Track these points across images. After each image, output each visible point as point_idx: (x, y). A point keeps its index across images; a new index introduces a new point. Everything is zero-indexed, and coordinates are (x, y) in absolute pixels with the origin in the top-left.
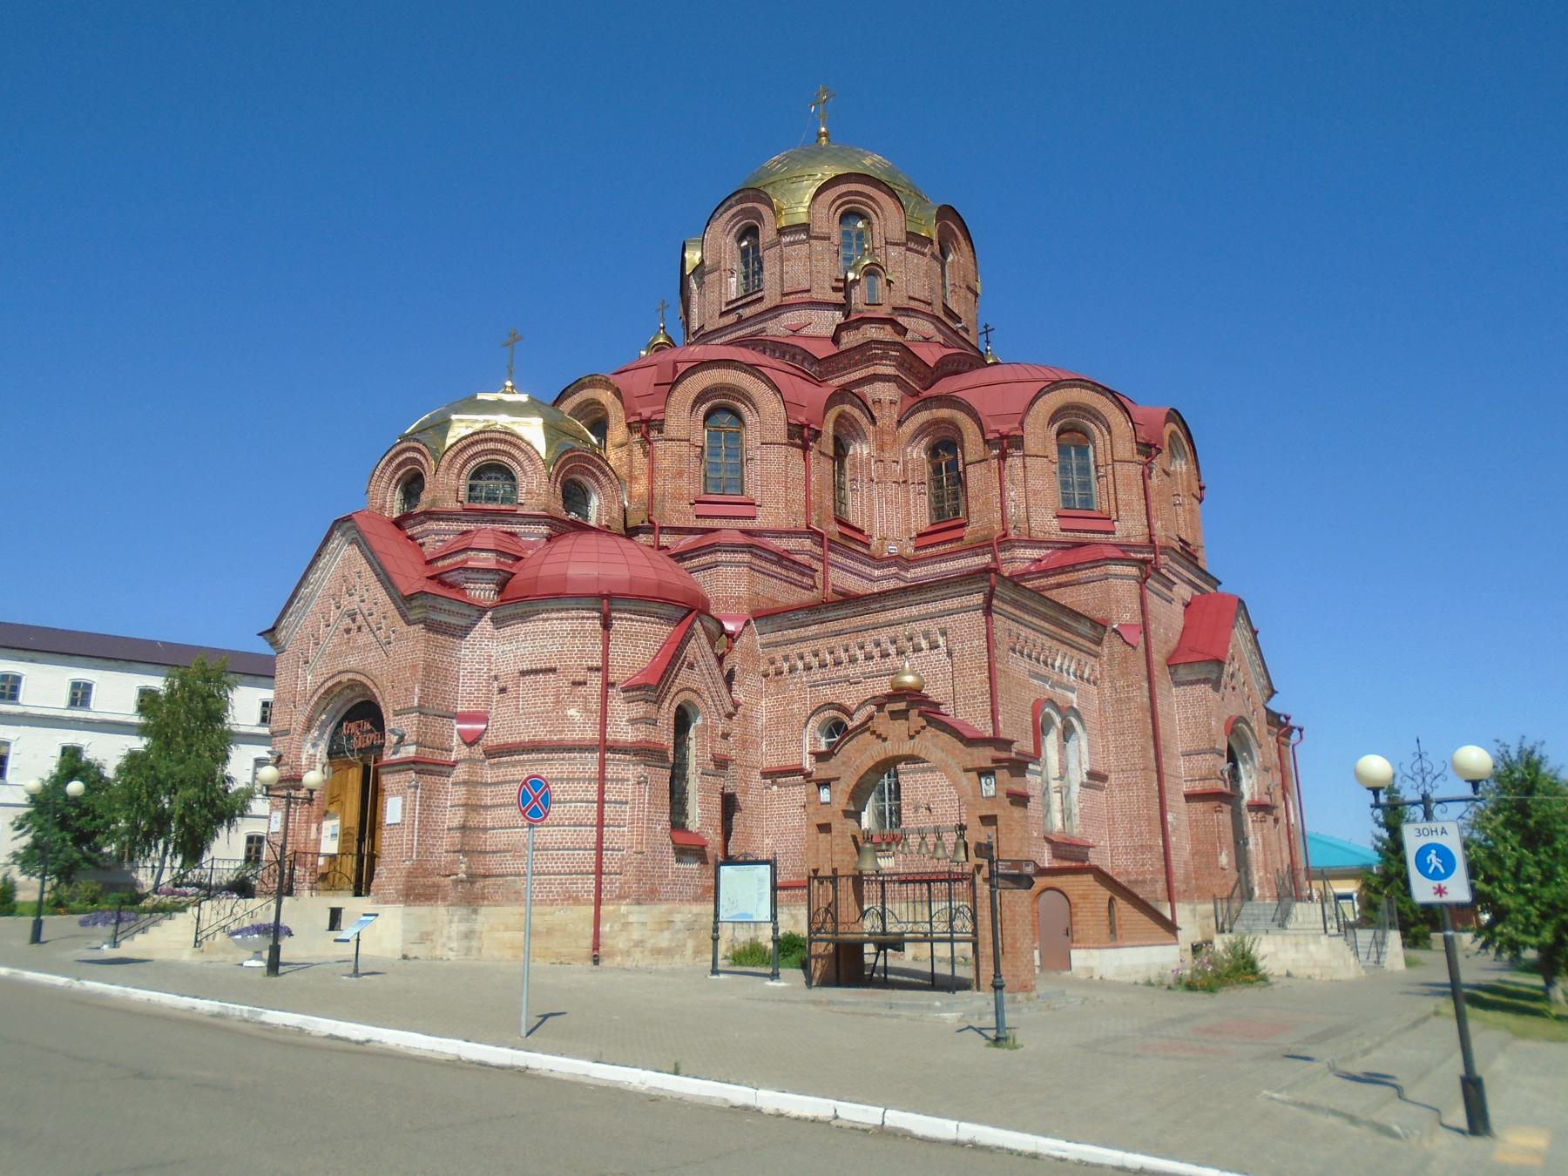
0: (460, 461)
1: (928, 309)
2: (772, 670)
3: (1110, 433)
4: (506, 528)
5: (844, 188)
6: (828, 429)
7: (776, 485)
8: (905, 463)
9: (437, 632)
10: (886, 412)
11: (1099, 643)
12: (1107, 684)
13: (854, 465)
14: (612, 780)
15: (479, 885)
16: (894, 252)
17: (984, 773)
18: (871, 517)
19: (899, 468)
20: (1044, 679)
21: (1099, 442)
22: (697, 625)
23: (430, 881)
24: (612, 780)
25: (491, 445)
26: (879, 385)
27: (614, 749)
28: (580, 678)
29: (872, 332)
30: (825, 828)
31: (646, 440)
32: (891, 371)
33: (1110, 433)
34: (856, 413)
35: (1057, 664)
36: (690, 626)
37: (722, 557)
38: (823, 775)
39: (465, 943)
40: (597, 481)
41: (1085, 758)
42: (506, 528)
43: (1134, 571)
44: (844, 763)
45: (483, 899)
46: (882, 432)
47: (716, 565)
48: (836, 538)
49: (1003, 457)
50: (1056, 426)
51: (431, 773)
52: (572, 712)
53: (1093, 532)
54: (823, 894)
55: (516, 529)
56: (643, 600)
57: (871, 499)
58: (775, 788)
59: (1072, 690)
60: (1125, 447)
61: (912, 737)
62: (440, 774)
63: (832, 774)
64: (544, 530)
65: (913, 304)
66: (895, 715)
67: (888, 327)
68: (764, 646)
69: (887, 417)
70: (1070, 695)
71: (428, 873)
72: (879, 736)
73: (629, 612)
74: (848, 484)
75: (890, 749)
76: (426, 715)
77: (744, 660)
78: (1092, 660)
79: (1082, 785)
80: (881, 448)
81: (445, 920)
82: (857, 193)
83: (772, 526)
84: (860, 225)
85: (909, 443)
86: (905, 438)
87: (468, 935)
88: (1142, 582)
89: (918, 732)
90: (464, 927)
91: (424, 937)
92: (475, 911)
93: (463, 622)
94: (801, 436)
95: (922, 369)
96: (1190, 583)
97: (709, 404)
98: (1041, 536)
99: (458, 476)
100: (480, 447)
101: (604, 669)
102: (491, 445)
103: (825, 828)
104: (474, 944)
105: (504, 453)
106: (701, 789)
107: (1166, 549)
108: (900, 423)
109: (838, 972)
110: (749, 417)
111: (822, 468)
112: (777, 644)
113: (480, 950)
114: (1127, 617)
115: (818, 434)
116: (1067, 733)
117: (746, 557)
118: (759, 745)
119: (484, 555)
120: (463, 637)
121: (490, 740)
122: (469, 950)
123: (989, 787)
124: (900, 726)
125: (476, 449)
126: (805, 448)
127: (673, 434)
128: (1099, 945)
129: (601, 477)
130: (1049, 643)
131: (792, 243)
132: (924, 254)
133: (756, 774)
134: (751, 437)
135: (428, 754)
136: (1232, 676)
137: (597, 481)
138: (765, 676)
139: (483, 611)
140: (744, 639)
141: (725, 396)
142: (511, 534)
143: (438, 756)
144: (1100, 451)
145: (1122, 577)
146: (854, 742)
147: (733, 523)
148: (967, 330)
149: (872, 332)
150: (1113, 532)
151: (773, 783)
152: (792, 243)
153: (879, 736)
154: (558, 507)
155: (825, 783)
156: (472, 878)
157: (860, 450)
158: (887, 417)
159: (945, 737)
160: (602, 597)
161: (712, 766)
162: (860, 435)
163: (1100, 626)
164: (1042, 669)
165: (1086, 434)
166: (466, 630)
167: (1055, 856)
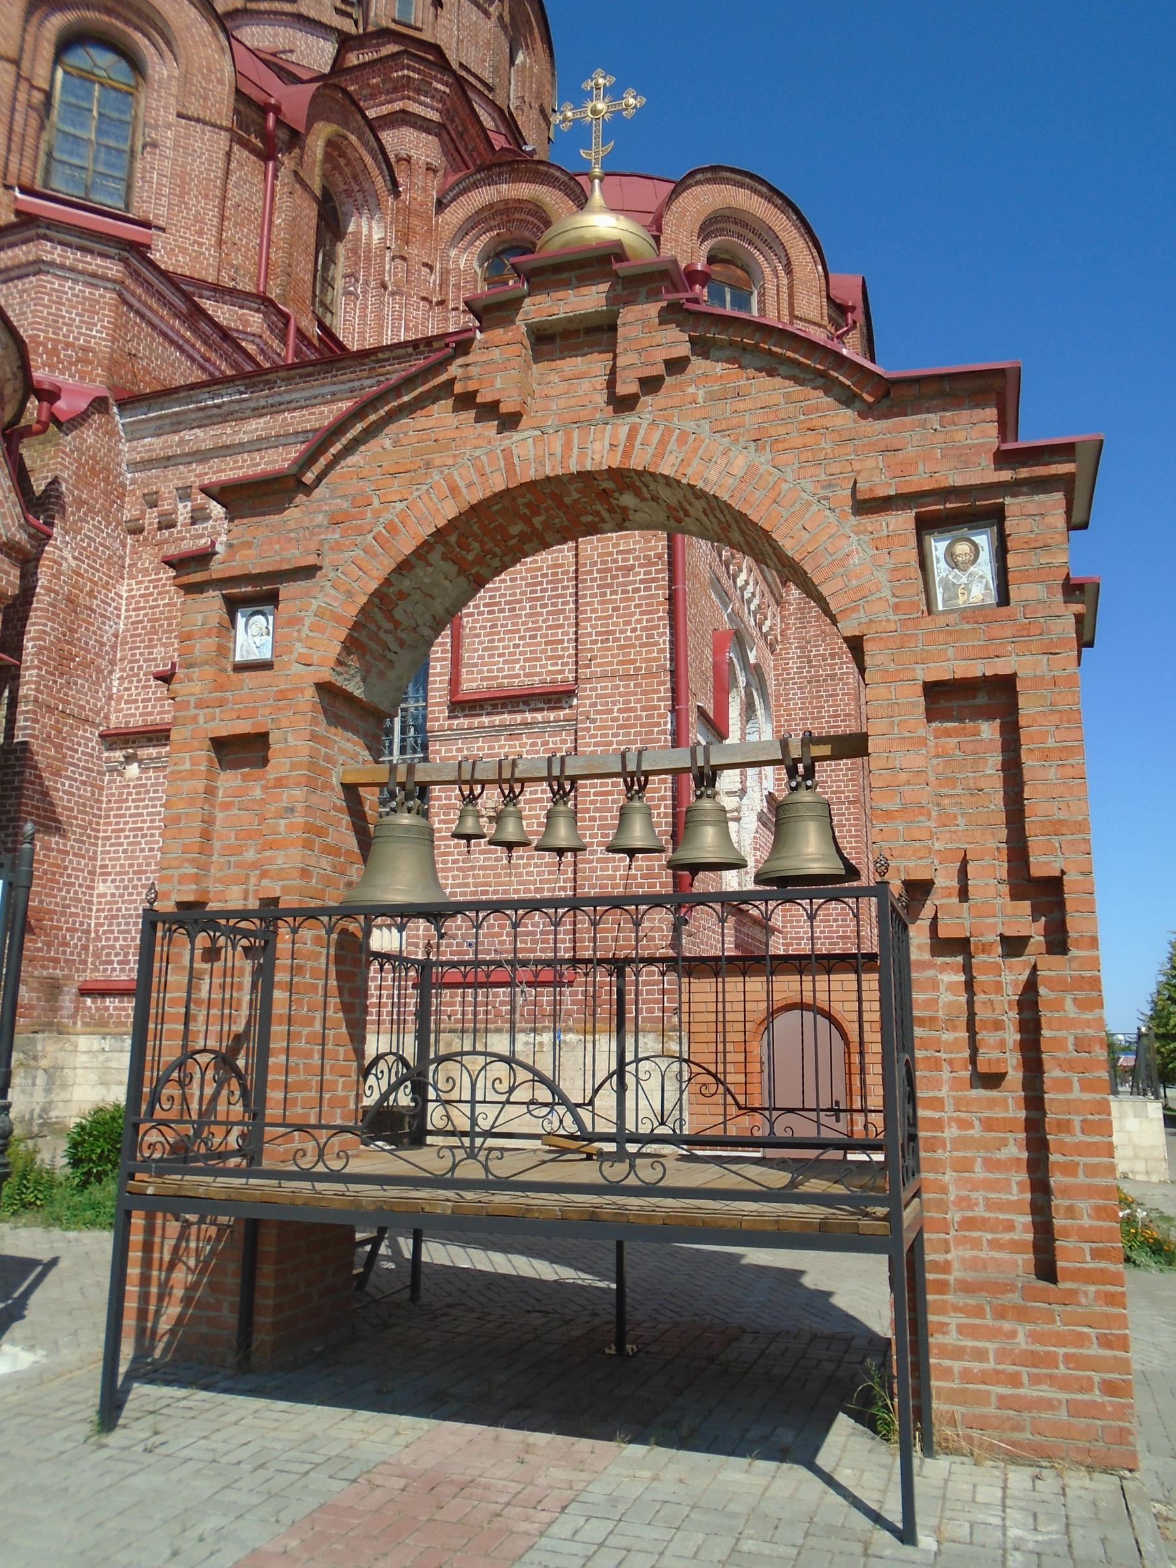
2: (151, 518)
3: (789, 272)
8: (445, 272)
10: (419, 180)
12: (793, 652)
13: (355, 251)
17: (946, 513)
19: (435, 278)
21: (771, 287)
30: (242, 750)
32: (435, 116)
33: (789, 272)
37: (51, 252)
38: (252, 562)
44: (336, 521)
46: (408, 211)
47: (38, 267)
50: (708, 244)
54: (209, 996)
57: (380, 318)
58: (133, 770)
61: (622, 404)
63: (297, 557)
66: (549, 341)
68: (134, 466)
69: (420, 190)
72: (489, 411)
74: (339, 284)
75: (534, 454)
77: (81, 480)
80: (405, 237)
85: (455, 240)
86: (447, 233)
89: (651, 385)
94: (260, 129)
95: (482, 146)
97: (71, 16)
103: (242, 750)
108: (441, 206)
109: (247, 1310)
110: (160, 68)
111: (295, 213)
112: (167, 461)
115: (296, 139)
117: (114, 269)
118: (102, 676)
123: (965, 572)
124: (584, 374)
126: (267, 155)
133: (93, 734)
134: (159, 104)
138: (136, 531)
140: (89, 435)
144: (771, 301)
146: (385, 440)
151: (129, 759)
153: (489, 411)
155: (256, 593)
157: (369, 230)
158: (420, 190)
159: (772, 391)
167: (737, 947)
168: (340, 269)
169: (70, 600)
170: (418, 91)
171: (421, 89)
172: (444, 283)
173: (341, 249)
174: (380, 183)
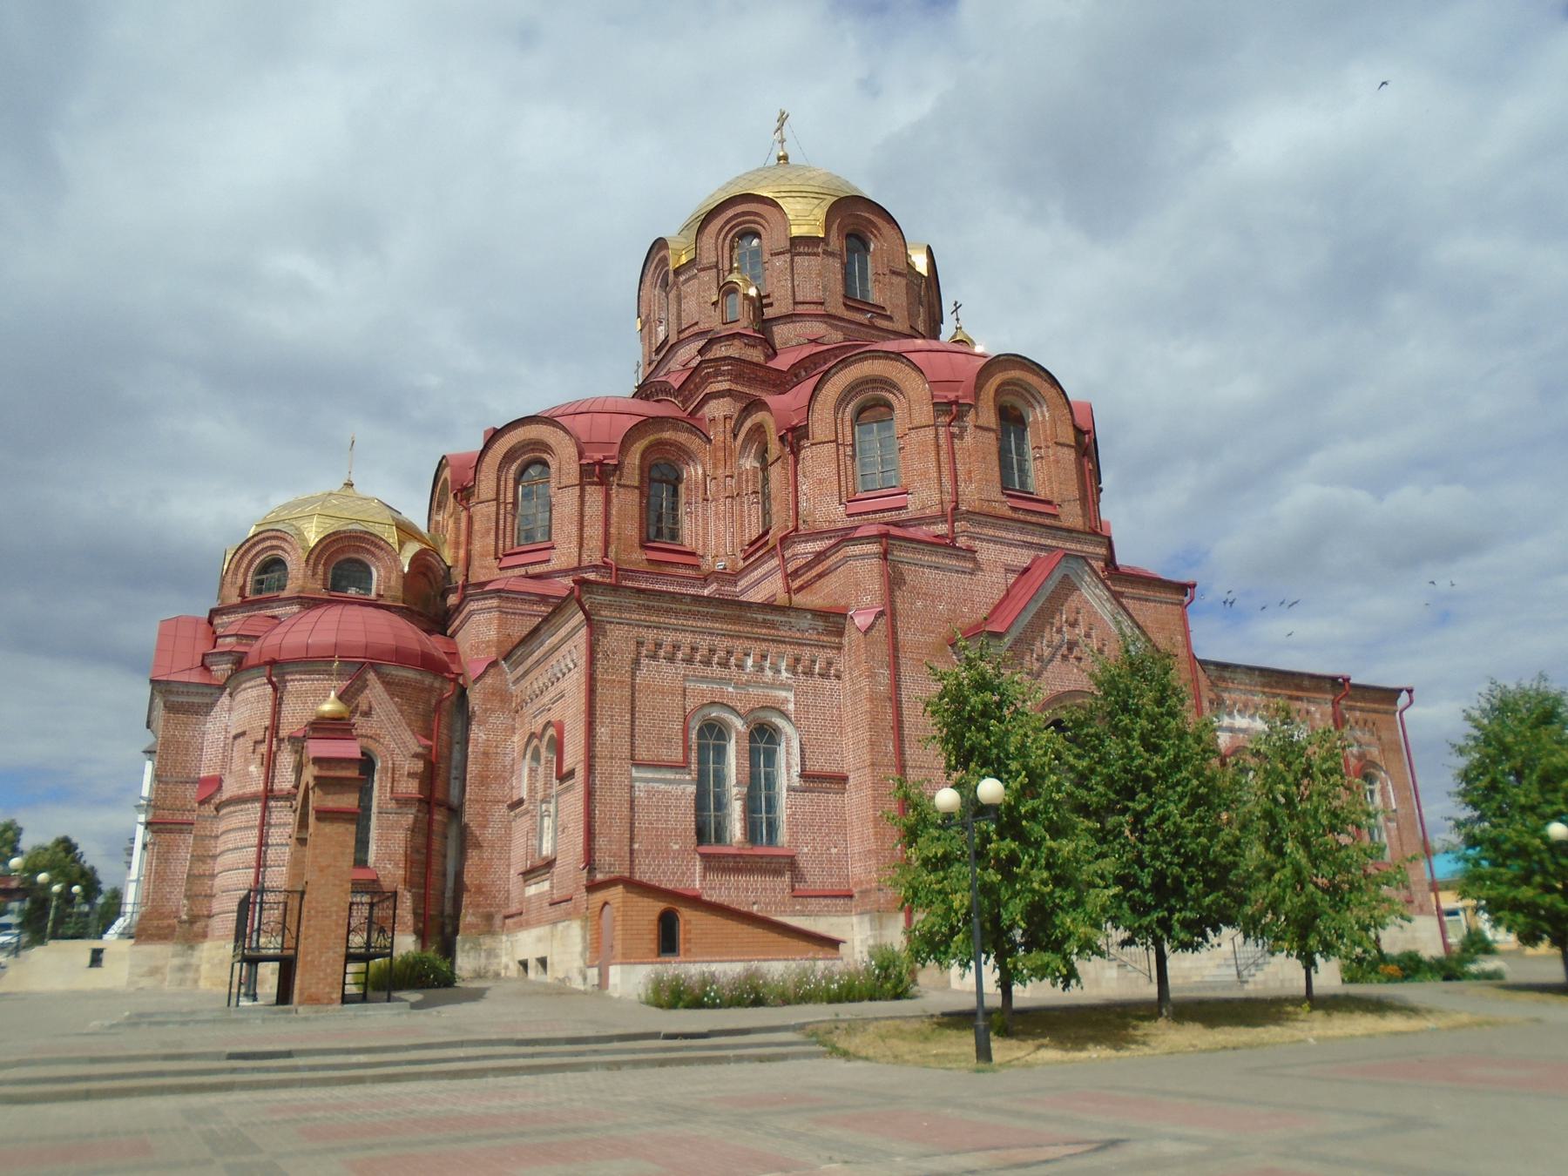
0: (246, 561)
1: (820, 310)
4: (269, 612)
5: (730, 213)
6: (634, 458)
7: (574, 525)
8: (740, 474)
9: (178, 712)
11: (841, 634)
14: (252, 827)
15: (198, 927)
16: (780, 262)
18: (706, 534)
20: (728, 681)
22: (371, 676)
23: (166, 922)
24: (252, 827)
25: (268, 543)
26: (713, 404)
27: (277, 798)
28: (260, 737)
29: (720, 351)
31: (467, 509)
32: (725, 386)
34: (682, 437)
35: (750, 662)
36: (358, 677)
39: (180, 975)
40: (373, 554)
41: (796, 759)
42: (269, 612)
43: (874, 548)
45: (204, 936)
48: (644, 567)
49: (796, 452)
51: (171, 832)
52: (252, 768)
53: (883, 511)
55: (277, 612)
56: (312, 662)
59: (784, 686)
60: (924, 413)
62: (181, 832)
64: (295, 608)
65: (800, 309)
67: (736, 342)
69: (718, 434)
70: (784, 694)
71: (162, 916)
73: (300, 673)
76: (167, 783)
77: (485, 701)
78: (831, 653)
79: (791, 789)
81: (162, 952)
82: (736, 216)
83: (564, 566)
84: (755, 242)
87: (183, 968)
88: (885, 556)
90: (177, 961)
91: (154, 971)
92: (192, 948)
93: (207, 700)
94: (597, 473)
96: (1029, 545)
98: (825, 527)
99: (246, 575)
100: (258, 548)
101: (274, 728)
102: (268, 543)
104: (190, 975)
105: (273, 548)
106: (380, 827)
107: (981, 517)
108: (735, 436)
111: (626, 502)
113: (196, 981)
114: (867, 599)
116: (763, 736)
117: (494, 602)
119: (228, 640)
120: (207, 714)
121: (226, 794)
122: (181, 982)
125: (258, 548)
126: (603, 481)
127: (483, 497)
128: (628, 958)
129: (377, 551)
130: (727, 643)
131: (687, 281)
132: (815, 254)
133: (503, 808)
135: (167, 816)
136: (1072, 645)
137: (373, 554)
139: (222, 688)
141: (533, 450)
142: (274, 617)
143: (178, 817)
145: (863, 556)
147: (517, 572)
148: (890, 318)
149: (720, 351)
150: (905, 507)
152: (687, 281)
154: (316, 588)
156: (193, 920)
160: (273, 663)
161: (393, 805)
162: (687, 455)
163: (833, 620)
164: (716, 671)
165: (890, 407)
166: (208, 708)
168: (683, 499)
169: (486, 754)
170: (716, 375)
171: (718, 373)
172: (739, 482)
173: (682, 488)
174: (694, 443)
